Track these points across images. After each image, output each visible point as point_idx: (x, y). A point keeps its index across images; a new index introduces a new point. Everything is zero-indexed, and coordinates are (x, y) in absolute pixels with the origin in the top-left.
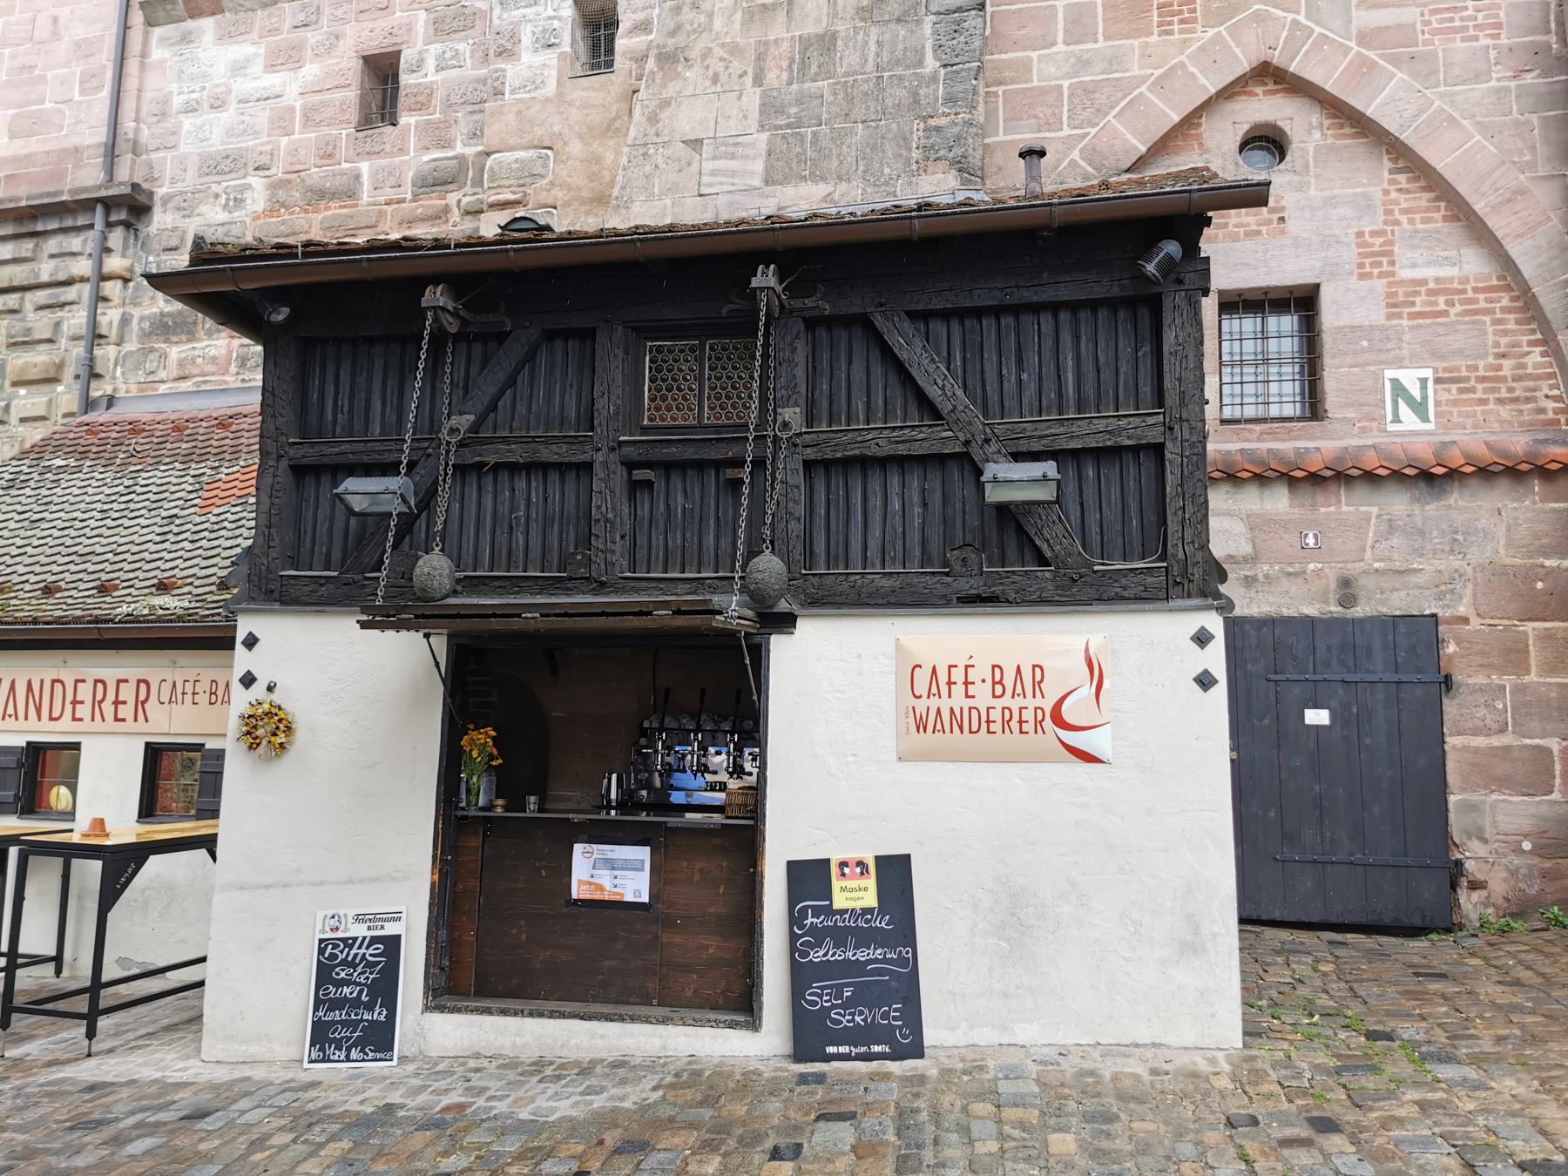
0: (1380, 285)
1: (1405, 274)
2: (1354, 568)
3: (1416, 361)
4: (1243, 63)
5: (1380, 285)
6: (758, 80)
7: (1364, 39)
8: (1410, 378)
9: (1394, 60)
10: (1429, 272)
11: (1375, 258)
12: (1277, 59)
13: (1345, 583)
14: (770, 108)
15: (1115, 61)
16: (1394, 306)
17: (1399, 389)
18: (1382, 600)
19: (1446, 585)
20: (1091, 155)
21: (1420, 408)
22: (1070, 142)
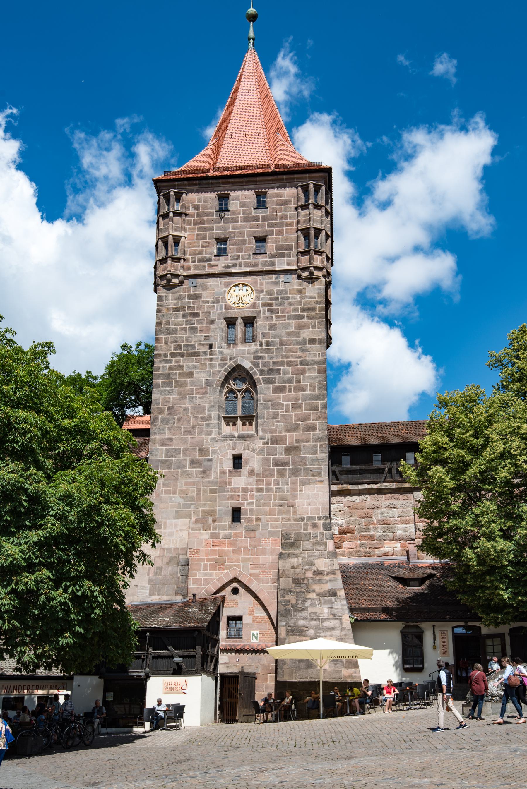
0: (251, 617)
1: (256, 615)
2: (244, 665)
3: (256, 630)
4: (231, 577)
5: (251, 617)
6: (148, 574)
7: (251, 575)
8: (255, 633)
9: (255, 579)
10: (259, 615)
11: (251, 612)
12: (237, 577)
13: (242, 667)
14: (150, 581)
15: (211, 575)
16: (254, 620)
17: (253, 635)
18: (248, 670)
19: (257, 667)
20: (206, 591)
21: (256, 638)
22: (203, 589)
